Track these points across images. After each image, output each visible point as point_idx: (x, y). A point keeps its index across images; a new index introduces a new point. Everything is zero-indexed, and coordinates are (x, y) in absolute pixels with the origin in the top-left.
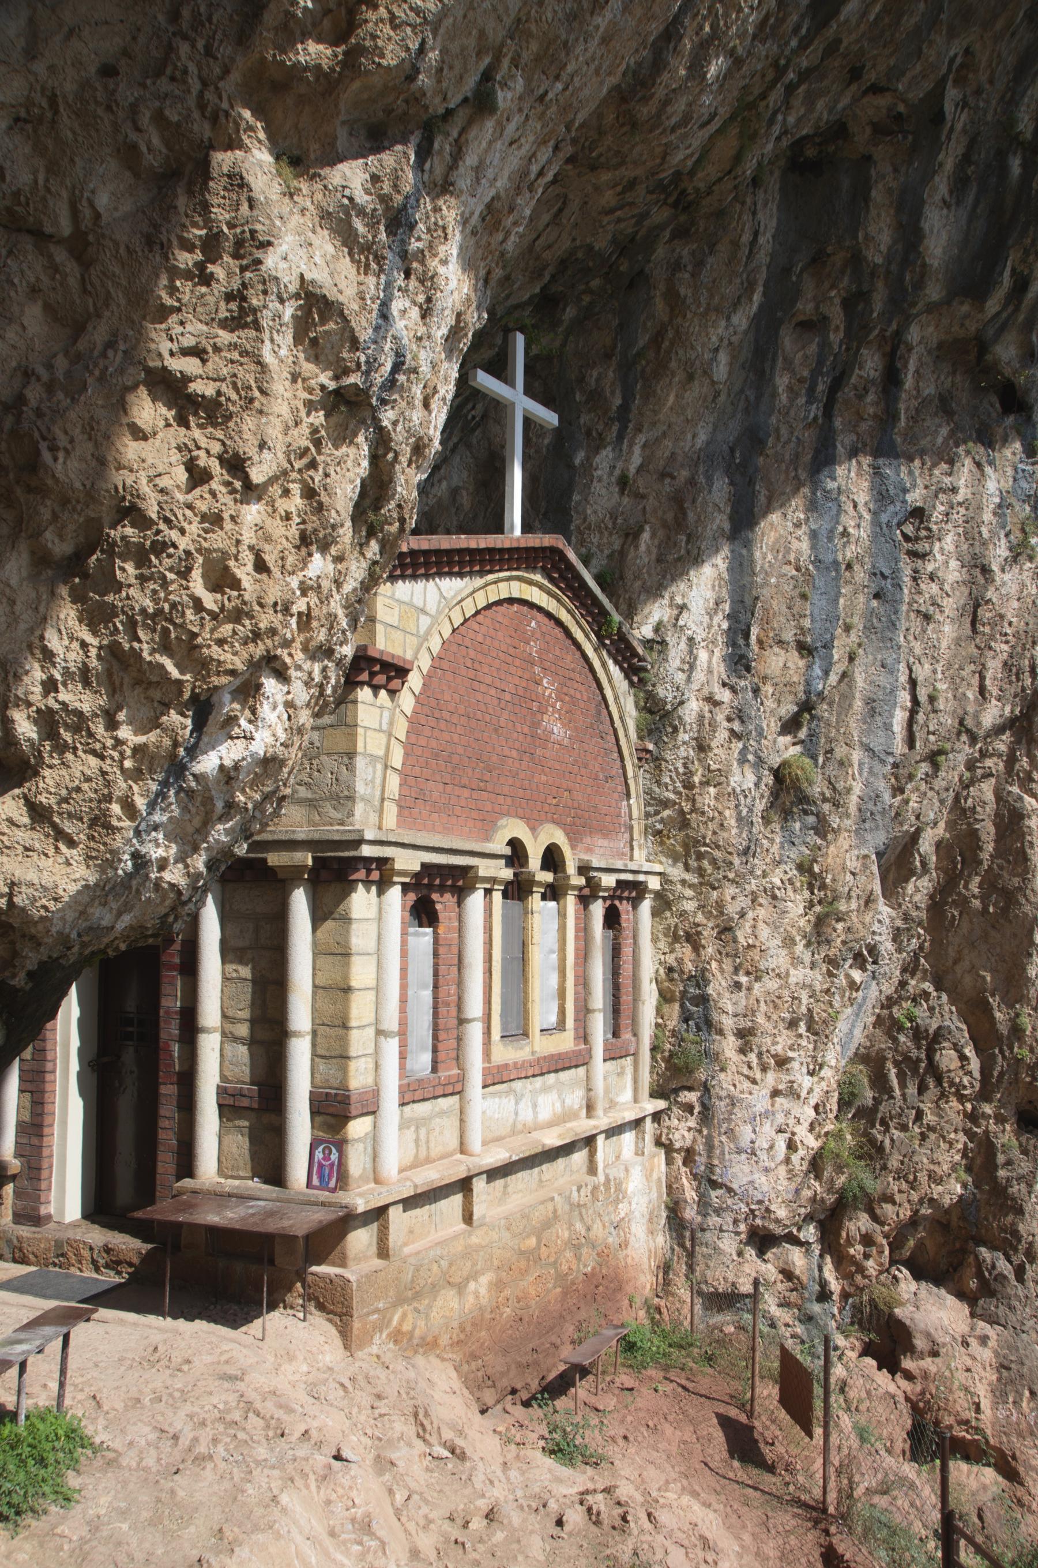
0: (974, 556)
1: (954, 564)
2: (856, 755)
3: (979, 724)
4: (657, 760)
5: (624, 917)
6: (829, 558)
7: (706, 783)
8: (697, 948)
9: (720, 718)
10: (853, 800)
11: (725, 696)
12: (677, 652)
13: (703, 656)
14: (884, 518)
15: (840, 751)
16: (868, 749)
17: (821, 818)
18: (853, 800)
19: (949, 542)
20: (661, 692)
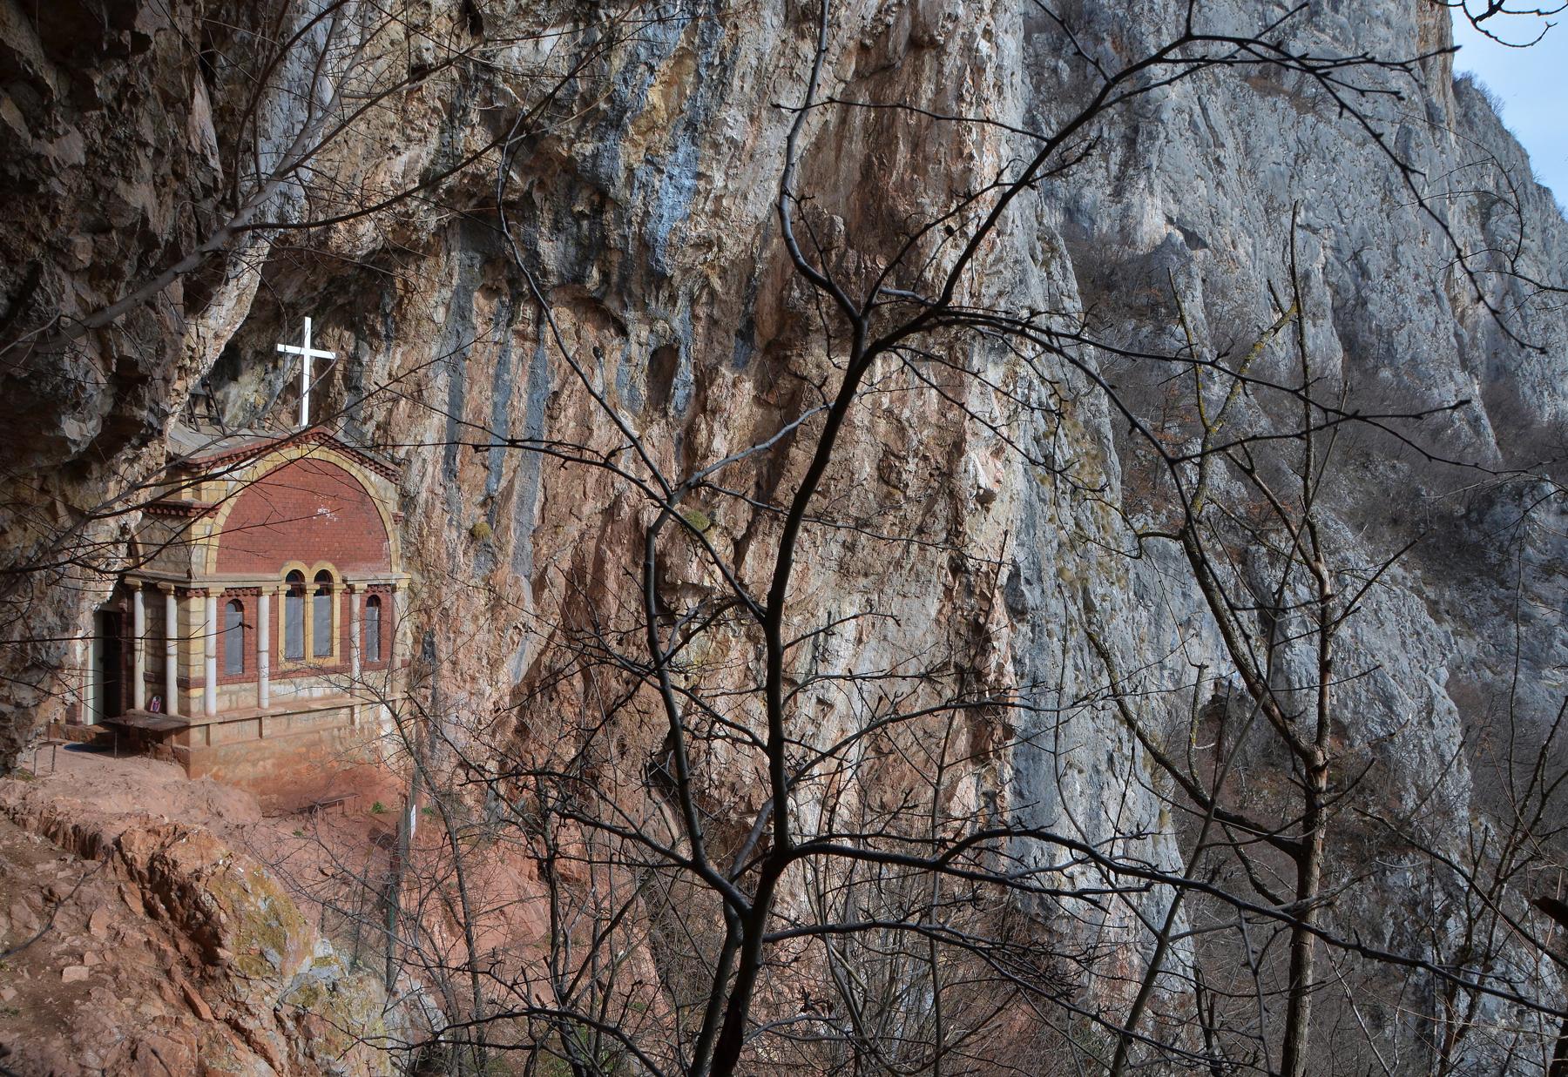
0: (583, 420)
1: (572, 424)
2: (513, 525)
3: (580, 512)
4: (407, 522)
5: (383, 601)
6: (501, 418)
7: (430, 534)
8: (430, 618)
9: (438, 504)
10: (510, 549)
11: (440, 491)
12: (416, 466)
13: (430, 469)
14: (535, 396)
15: (504, 521)
16: (518, 521)
17: (493, 555)
18: (510, 549)
19: (571, 412)
20: (407, 486)
